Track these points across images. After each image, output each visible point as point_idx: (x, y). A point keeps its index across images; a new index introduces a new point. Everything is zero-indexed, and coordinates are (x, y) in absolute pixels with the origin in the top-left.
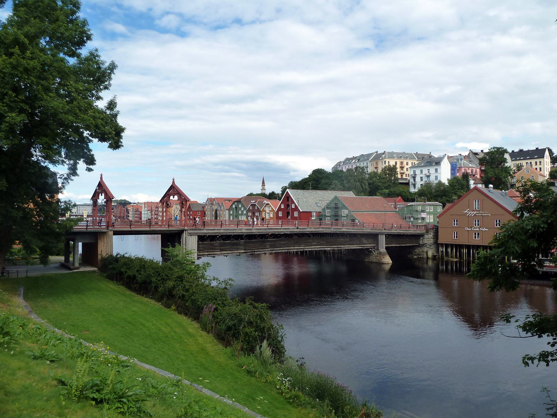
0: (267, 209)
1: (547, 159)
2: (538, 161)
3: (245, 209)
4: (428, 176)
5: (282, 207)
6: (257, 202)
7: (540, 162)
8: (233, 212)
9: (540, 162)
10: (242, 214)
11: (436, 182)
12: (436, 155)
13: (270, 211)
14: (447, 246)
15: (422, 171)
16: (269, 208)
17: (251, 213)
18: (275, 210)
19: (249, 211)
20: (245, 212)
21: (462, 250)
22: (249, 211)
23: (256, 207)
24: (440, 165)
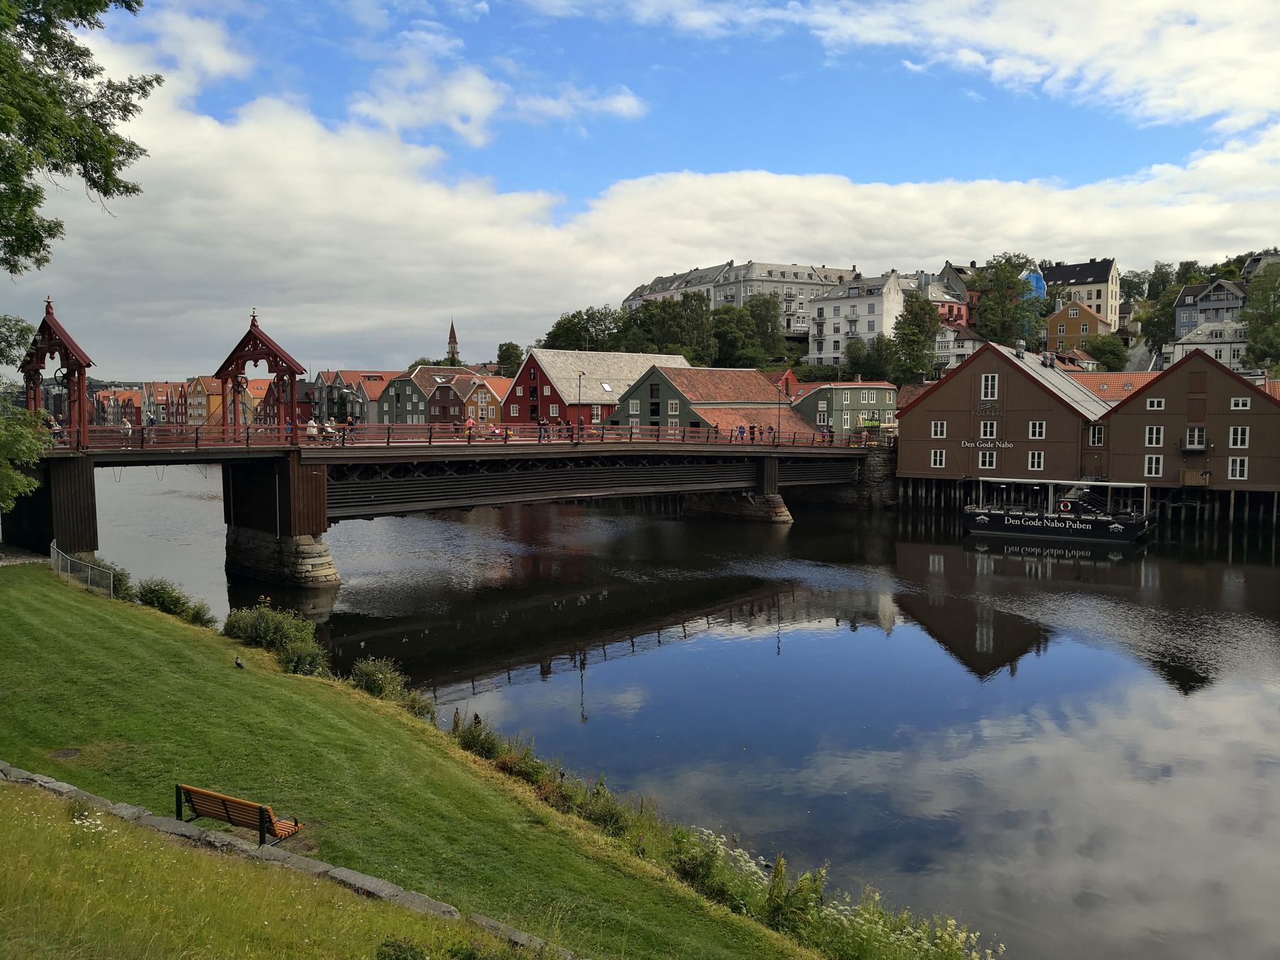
1: (1113, 287)
2: (1094, 288)
3: (422, 397)
4: (853, 322)
5: (518, 395)
6: (453, 382)
7: (1099, 292)
9: (1099, 292)
10: (415, 411)
11: (873, 335)
12: (870, 271)
13: (489, 404)
14: (916, 482)
15: (837, 310)
16: (484, 396)
17: (437, 409)
19: (431, 402)
20: (421, 407)
21: (952, 492)
24: (881, 295)
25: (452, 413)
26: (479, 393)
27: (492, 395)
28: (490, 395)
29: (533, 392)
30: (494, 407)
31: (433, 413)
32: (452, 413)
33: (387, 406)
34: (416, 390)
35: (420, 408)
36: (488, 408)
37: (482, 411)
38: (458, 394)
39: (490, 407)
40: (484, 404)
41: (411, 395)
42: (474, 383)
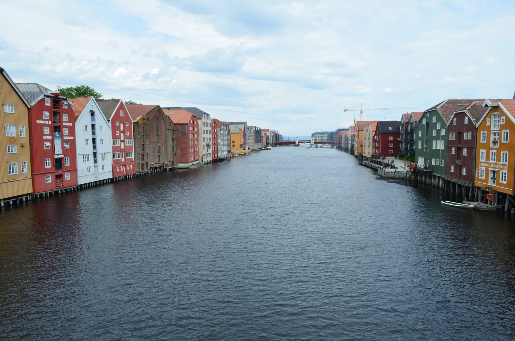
0: (493, 121)
3: (443, 125)
6: (468, 108)
8: (423, 134)
10: (438, 137)
13: (502, 127)
16: (497, 119)
17: (454, 135)
19: (450, 129)
20: (443, 133)
22: (450, 129)
23: (466, 119)
25: (465, 139)
26: (493, 117)
27: (507, 118)
28: (504, 117)
31: (450, 139)
32: (465, 139)
34: (439, 119)
35: (442, 135)
36: (501, 132)
37: (495, 135)
38: (472, 119)
39: (503, 131)
41: (436, 124)
42: (486, 105)
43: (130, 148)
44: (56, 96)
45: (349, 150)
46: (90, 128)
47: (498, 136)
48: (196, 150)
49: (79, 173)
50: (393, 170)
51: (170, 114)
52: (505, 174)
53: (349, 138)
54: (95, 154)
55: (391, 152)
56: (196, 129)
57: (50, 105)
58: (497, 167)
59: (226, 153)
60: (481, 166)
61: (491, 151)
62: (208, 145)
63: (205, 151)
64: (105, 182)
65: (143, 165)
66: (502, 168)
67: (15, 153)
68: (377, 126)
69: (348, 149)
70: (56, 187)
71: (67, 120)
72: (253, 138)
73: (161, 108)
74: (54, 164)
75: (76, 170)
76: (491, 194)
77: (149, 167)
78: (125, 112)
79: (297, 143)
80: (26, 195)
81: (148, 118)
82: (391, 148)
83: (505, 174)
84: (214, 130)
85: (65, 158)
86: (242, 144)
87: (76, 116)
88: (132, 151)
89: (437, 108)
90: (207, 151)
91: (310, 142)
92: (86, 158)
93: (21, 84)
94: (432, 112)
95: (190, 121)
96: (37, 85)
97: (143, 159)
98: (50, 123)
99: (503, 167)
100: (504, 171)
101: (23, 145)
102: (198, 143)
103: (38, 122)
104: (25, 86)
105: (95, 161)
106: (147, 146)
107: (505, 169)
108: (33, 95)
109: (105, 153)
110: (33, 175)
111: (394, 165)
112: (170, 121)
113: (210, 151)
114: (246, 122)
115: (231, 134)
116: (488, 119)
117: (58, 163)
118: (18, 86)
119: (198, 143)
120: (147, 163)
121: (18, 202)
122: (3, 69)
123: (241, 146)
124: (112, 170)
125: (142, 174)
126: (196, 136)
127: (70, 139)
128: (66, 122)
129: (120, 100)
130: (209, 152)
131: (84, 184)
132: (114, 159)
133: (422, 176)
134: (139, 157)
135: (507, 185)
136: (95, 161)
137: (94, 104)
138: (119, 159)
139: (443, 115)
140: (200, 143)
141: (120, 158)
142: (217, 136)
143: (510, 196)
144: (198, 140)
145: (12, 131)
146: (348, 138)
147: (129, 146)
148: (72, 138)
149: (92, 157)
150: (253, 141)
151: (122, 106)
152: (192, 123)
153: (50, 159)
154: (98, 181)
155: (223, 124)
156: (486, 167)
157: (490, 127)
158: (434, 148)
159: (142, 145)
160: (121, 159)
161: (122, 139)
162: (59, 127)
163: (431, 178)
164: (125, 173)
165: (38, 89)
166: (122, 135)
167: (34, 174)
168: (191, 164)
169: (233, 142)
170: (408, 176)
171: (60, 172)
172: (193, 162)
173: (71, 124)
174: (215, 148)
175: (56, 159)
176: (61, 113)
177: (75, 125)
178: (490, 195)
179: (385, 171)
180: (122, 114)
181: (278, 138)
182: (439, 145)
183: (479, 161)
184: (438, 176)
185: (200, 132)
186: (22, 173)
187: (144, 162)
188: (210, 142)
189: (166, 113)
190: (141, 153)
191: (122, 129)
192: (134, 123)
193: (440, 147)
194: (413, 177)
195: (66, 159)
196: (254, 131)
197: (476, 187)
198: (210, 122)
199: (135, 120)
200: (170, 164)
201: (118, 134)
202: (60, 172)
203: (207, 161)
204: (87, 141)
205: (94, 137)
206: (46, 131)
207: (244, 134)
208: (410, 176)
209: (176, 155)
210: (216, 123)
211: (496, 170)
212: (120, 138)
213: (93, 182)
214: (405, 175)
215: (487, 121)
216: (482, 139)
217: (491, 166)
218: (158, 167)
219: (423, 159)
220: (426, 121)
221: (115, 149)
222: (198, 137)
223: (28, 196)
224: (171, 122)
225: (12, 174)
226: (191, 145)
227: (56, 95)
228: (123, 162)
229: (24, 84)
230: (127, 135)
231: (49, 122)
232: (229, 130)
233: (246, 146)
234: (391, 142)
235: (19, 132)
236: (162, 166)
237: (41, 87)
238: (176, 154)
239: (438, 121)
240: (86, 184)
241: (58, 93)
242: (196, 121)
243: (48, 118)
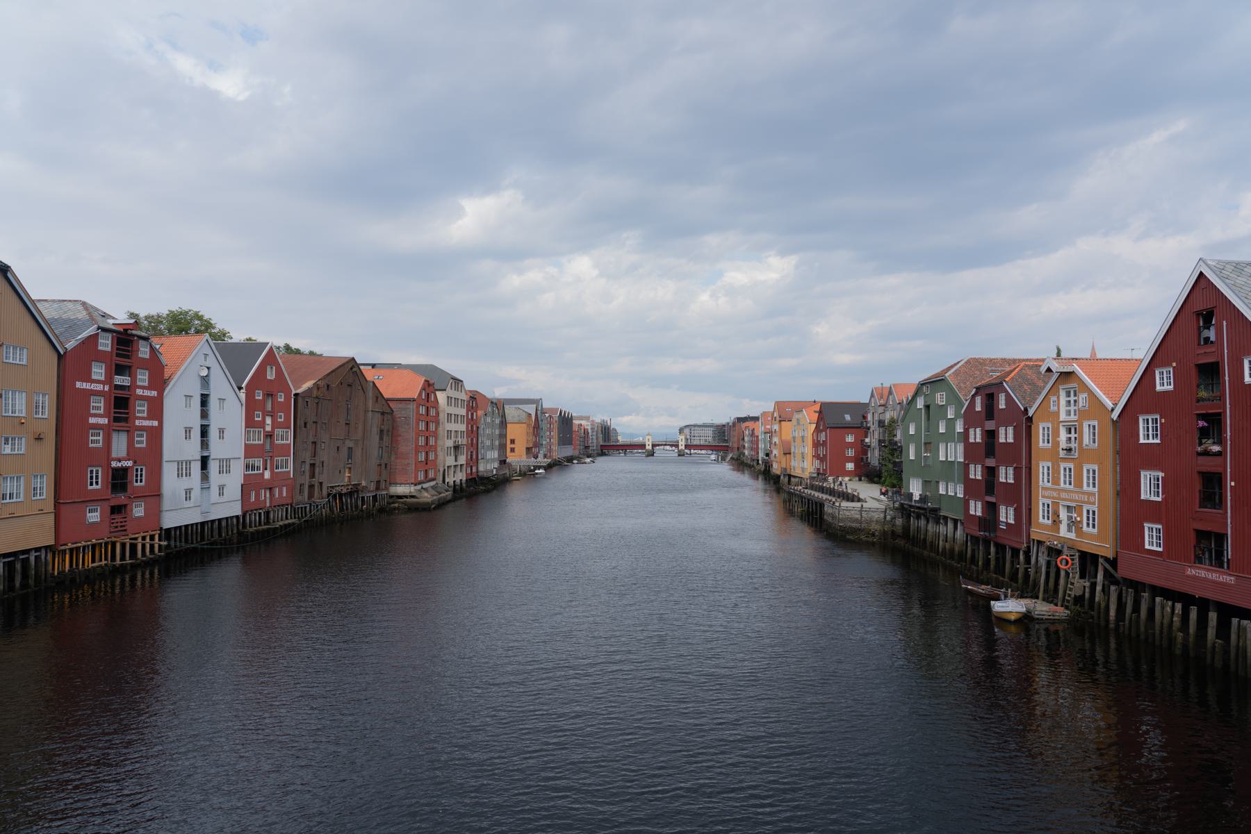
8: (918, 429)
10: (949, 437)
13: (1083, 415)
16: (1072, 398)
18: (1109, 404)
20: (959, 428)
26: (1063, 394)
27: (1092, 394)
29: (1210, 372)
30: (1096, 423)
33: (914, 429)
35: (959, 431)
36: (1081, 426)
40: (1073, 417)
42: (1049, 370)
43: (284, 450)
44: (126, 330)
45: (760, 462)
46: (197, 401)
47: (1076, 433)
48: (432, 456)
49: (167, 503)
50: (858, 505)
51: (377, 377)
52: (1094, 512)
53: (760, 438)
54: (204, 462)
55: (850, 466)
56: (432, 412)
57: (109, 349)
58: (1077, 498)
59: (496, 465)
60: (1043, 497)
61: (1063, 465)
62: (456, 448)
63: (450, 461)
64: (224, 523)
65: (311, 487)
66: (1086, 500)
67: (20, 452)
68: (820, 412)
69: (758, 460)
70: (111, 532)
71: (146, 384)
72: (555, 434)
73: (358, 365)
74: (110, 479)
75: (159, 495)
76: (1065, 557)
77: (325, 492)
78: (279, 372)
79: (649, 447)
80: (38, 549)
81: (328, 386)
82: (849, 460)
83: (1094, 512)
84: (472, 414)
85: (135, 468)
86: (531, 446)
87: (166, 376)
88: (290, 456)
89: (947, 375)
90: (456, 460)
91: (677, 446)
92: (183, 469)
93: (46, 300)
94: (936, 382)
95: (420, 394)
96: (84, 304)
97: (313, 476)
98: (107, 388)
99: (1088, 498)
100: (1092, 508)
101: (41, 437)
102: (436, 442)
103: (78, 385)
104: (56, 306)
105: (205, 477)
106: (323, 445)
107: (1094, 503)
108: (73, 326)
109: (228, 460)
110: (57, 504)
111: (858, 493)
112: (377, 392)
113: (462, 460)
114: (541, 399)
115: (508, 425)
116: (1053, 398)
117: (119, 479)
118: (39, 305)
119: (436, 442)
120: (321, 484)
121: (18, 566)
122: (9, 267)
123: (528, 450)
124: (240, 498)
125: (308, 509)
126: (432, 427)
127: (150, 425)
128: (143, 388)
129: (268, 343)
130: (459, 463)
131: (176, 528)
132: (248, 472)
133: (918, 517)
134: (303, 469)
135: (1098, 537)
136: (205, 477)
137: (209, 352)
138: (258, 472)
139: (960, 388)
140: (439, 442)
141: (261, 471)
142: (478, 428)
143: (1107, 559)
144: (435, 435)
145: (18, 405)
146: (757, 437)
147: (283, 444)
148: (156, 423)
149: (196, 467)
150: (555, 441)
151: (271, 358)
152: (423, 397)
153: (100, 470)
154: (208, 522)
155: (492, 402)
156: (1053, 498)
157: (1058, 413)
158: (942, 458)
159: (312, 443)
160: (263, 474)
161: (268, 428)
162: (127, 399)
163: (938, 523)
164: (268, 505)
165: (85, 313)
166: (269, 420)
167: (61, 501)
168: (419, 487)
169: (513, 441)
170: (888, 518)
171: (121, 499)
172: (424, 483)
173: (154, 393)
174: (471, 455)
175: (116, 470)
176: (133, 369)
177: (163, 394)
178: (1063, 559)
179: (840, 506)
180: (271, 375)
181: (608, 437)
182: (953, 452)
183: (1039, 486)
184: (952, 519)
185: (443, 417)
186: (33, 498)
187: (315, 481)
188: (463, 441)
189: (369, 374)
190: (308, 462)
191: (269, 407)
192: (296, 395)
193: (956, 457)
194: (899, 522)
195: (137, 470)
196: (557, 419)
197: (1034, 540)
198: (464, 396)
199: (300, 387)
200: (372, 486)
201: (260, 419)
202: (121, 499)
203: (454, 482)
204: (188, 431)
205: (205, 423)
206: (98, 405)
207: (536, 428)
208: (893, 518)
209: (386, 467)
210: (474, 400)
211: (1073, 504)
212: (264, 428)
213: (197, 524)
214: (882, 515)
215: (1052, 402)
216: (1041, 441)
217: (1063, 495)
218: (345, 494)
219: (920, 483)
220: (925, 402)
221: (250, 451)
222: (436, 429)
223: (43, 551)
224: (378, 395)
225: (8, 501)
226: (421, 446)
227: (126, 327)
228: (266, 480)
229: (54, 301)
230: (279, 420)
231: (104, 388)
232: (504, 416)
233: (539, 451)
234: (850, 445)
235: (33, 407)
236: (355, 491)
237: (91, 310)
238: (386, 464)
239: (948, 403)
240: (180, 527)
241: (130, 324)
242: (433, 395)
243: (103, 378)
